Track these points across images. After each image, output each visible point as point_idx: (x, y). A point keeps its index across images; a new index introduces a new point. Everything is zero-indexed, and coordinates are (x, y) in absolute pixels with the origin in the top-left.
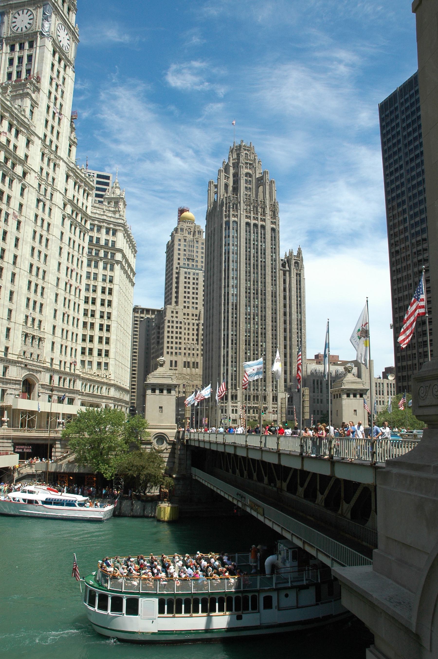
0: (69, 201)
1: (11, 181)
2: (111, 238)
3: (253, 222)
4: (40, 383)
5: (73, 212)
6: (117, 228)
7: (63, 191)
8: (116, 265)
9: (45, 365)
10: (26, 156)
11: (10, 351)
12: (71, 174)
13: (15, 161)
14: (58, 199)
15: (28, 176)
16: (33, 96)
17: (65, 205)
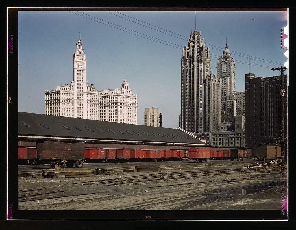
3: (189, 68)
7: (86, 99)
14: (85, 102)
15: (74, 101)
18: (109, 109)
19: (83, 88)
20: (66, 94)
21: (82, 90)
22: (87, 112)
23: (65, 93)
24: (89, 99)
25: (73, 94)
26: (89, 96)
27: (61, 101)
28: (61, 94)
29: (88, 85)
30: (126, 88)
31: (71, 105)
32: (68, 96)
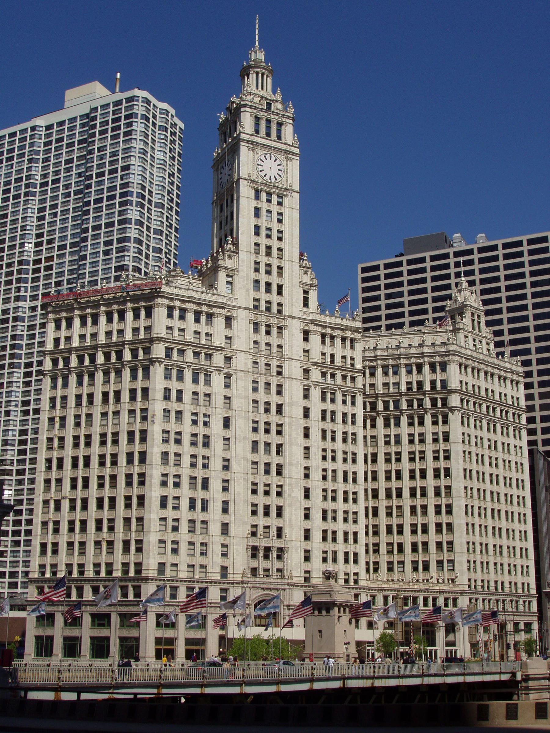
0: (315, 364)
1: (208, 376)
2: (439, 376)
4: (285, 604)
5: (324, 374)
6: (446, 359)
8: (450, 414)
9: (290, 581)
10: (228, 338)
11: (230, 570)
12: (311, 327)
13: (209, 352)
14: (294, 369)
15: (234, 360)
16: (229, 263)
17: (306, 371)
18: (393, 431)
19: (285, 290)
20: (190, 317)
21: (280, 299)
22: (307, 436)
23: (187, 306)
24: (316, 357)
25: (229, 320)
26: (315, 339)
27: (158, 351)
28: (164, 312)
29: (306, 279)
30: (473, 321)
31: (218, 380)
32: (203, 328)
